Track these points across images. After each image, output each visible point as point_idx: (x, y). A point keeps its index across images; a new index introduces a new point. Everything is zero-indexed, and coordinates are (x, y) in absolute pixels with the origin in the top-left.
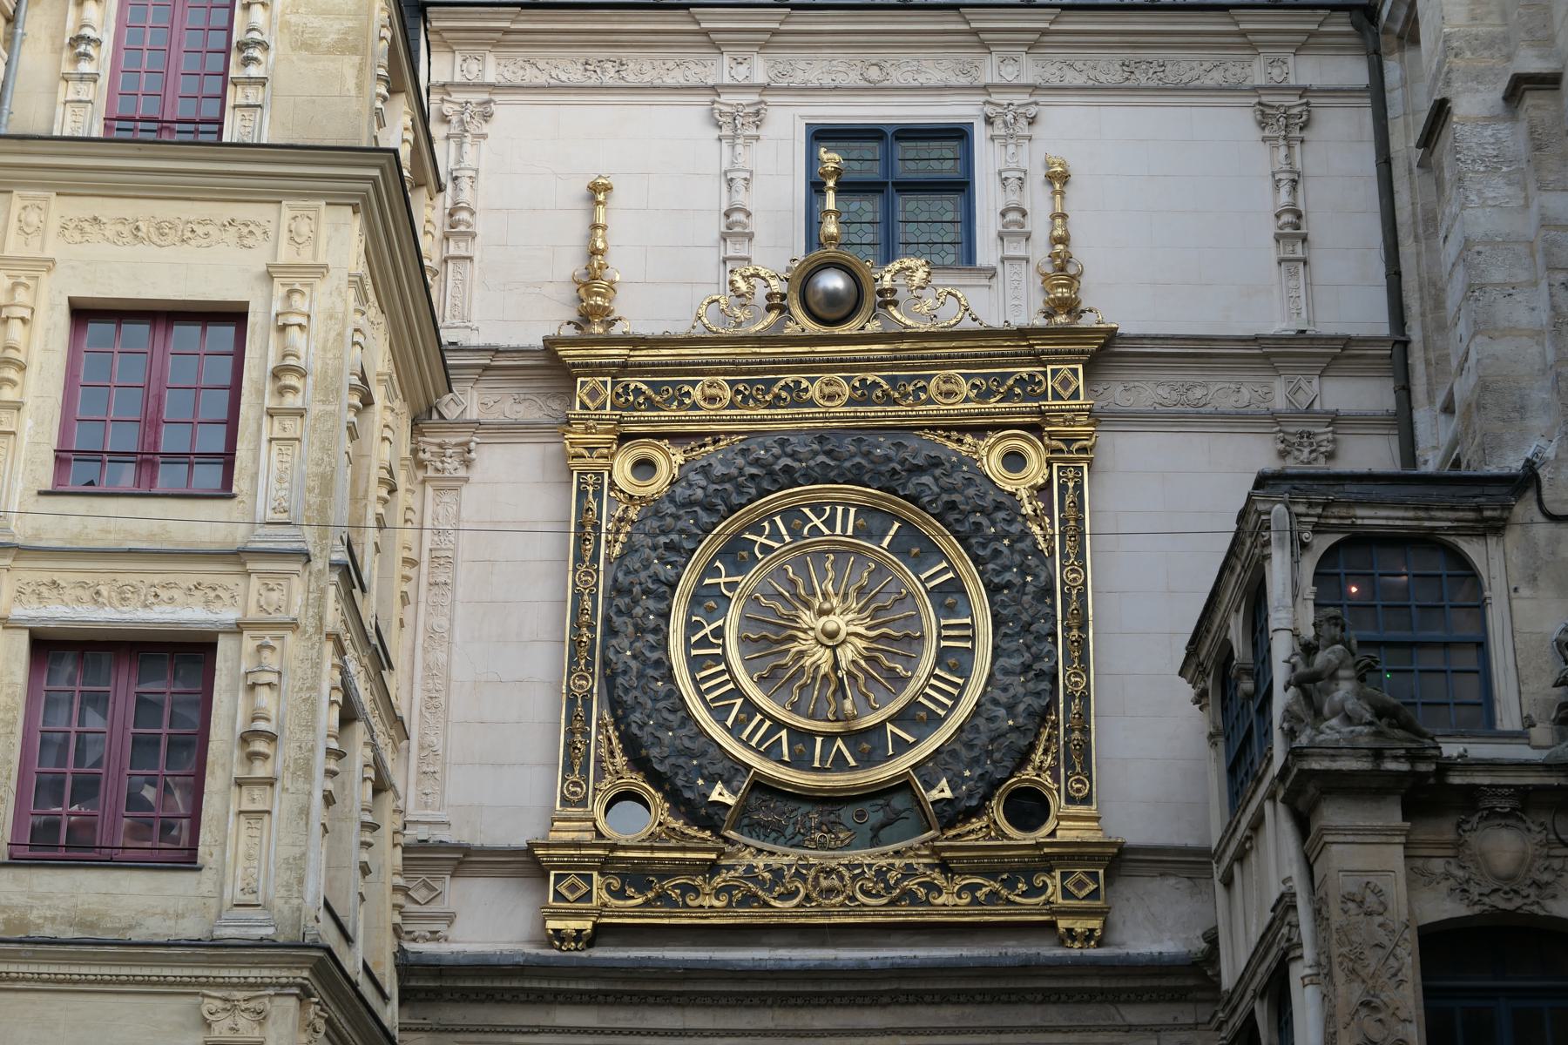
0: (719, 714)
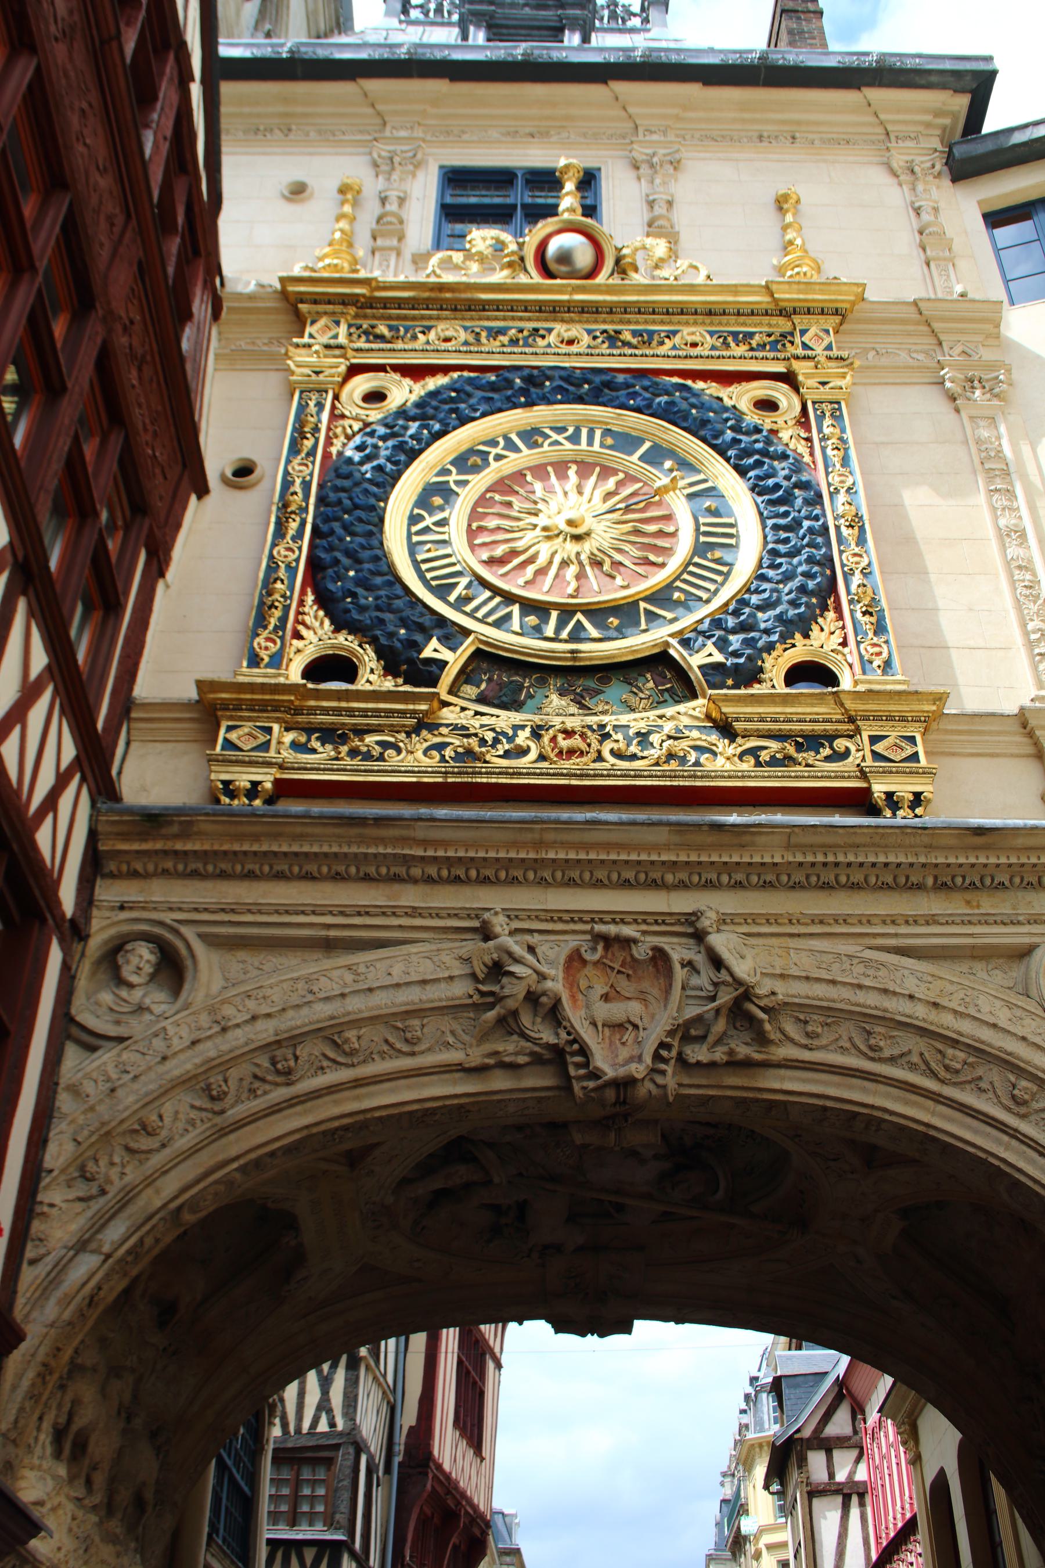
0: (442, 591)
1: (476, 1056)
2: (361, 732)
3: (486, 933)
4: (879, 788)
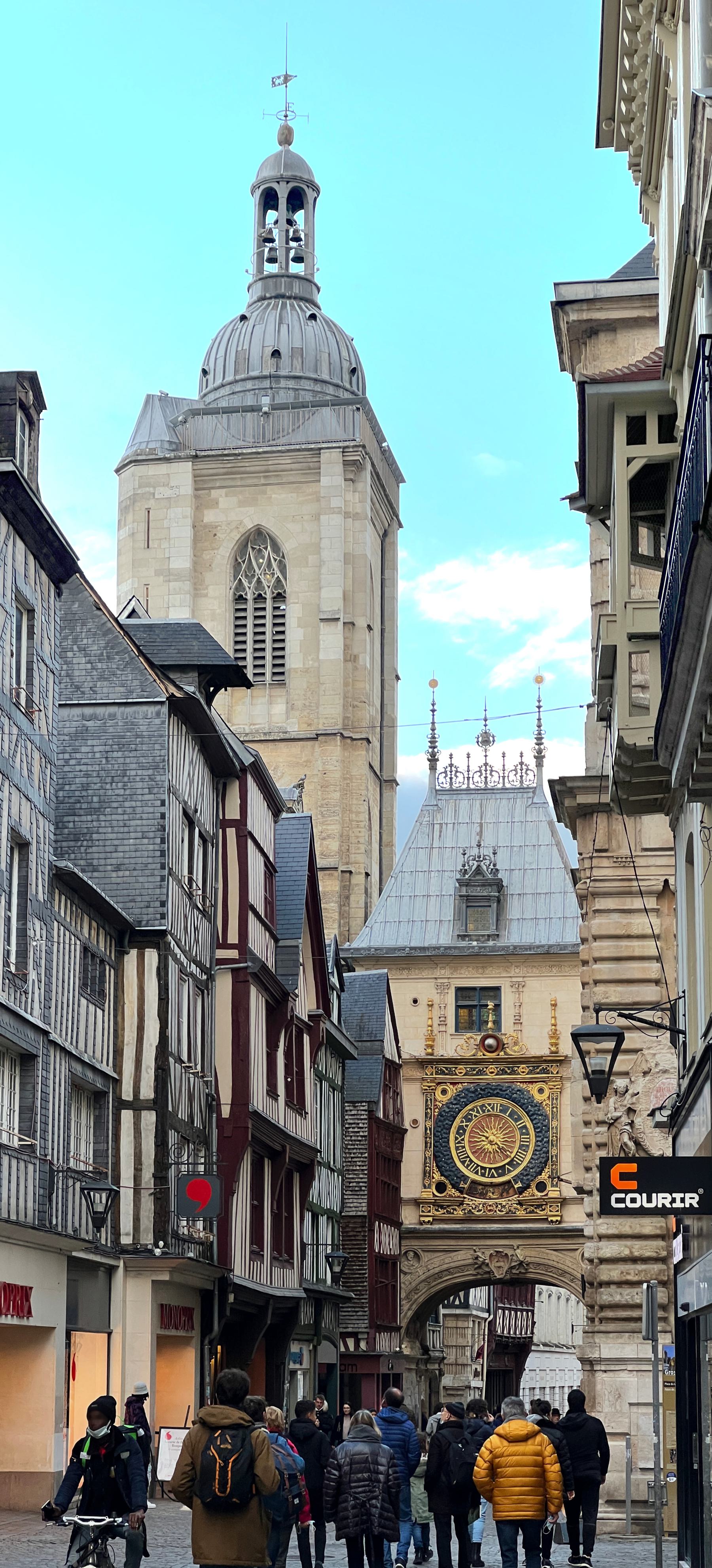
0: (463, 1163)
1: (474, 1273)
2: (448, 1206)
3: (475, 1251)
4: (550, 1219)
